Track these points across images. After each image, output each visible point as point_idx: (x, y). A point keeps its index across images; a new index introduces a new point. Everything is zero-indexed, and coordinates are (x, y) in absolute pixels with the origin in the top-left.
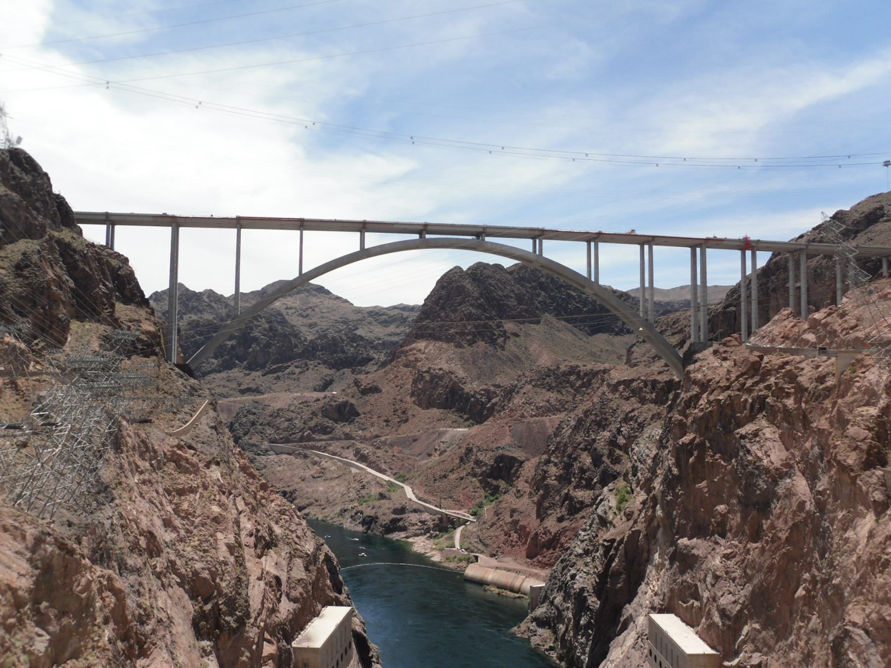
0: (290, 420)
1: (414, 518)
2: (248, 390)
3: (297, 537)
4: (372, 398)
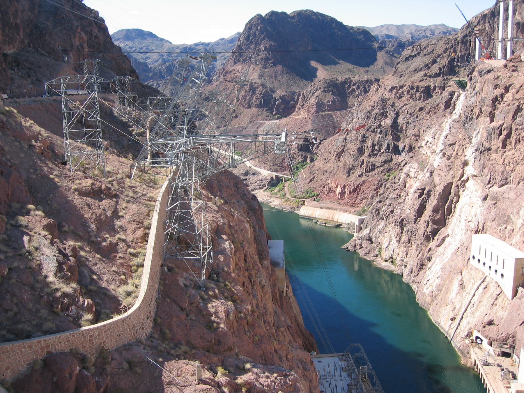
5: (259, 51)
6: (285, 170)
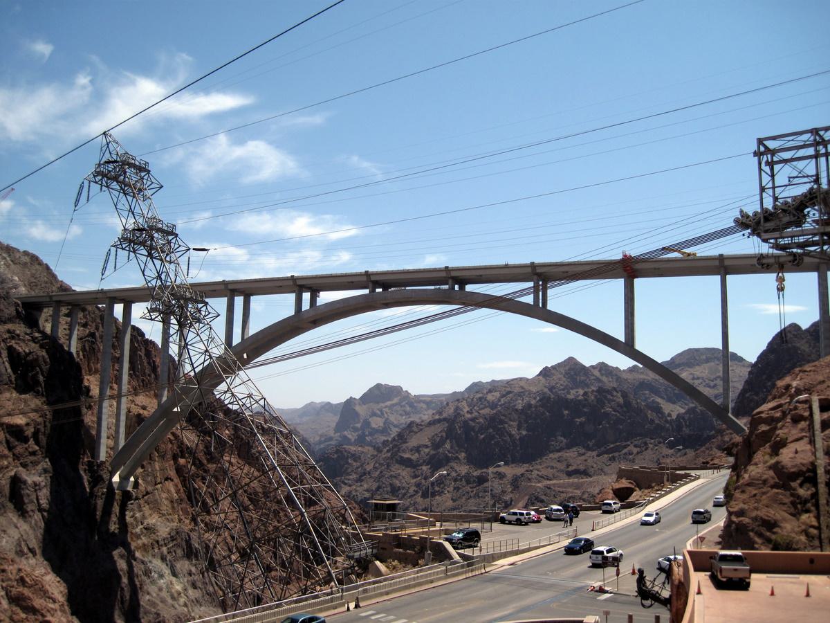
2: (577, 472)
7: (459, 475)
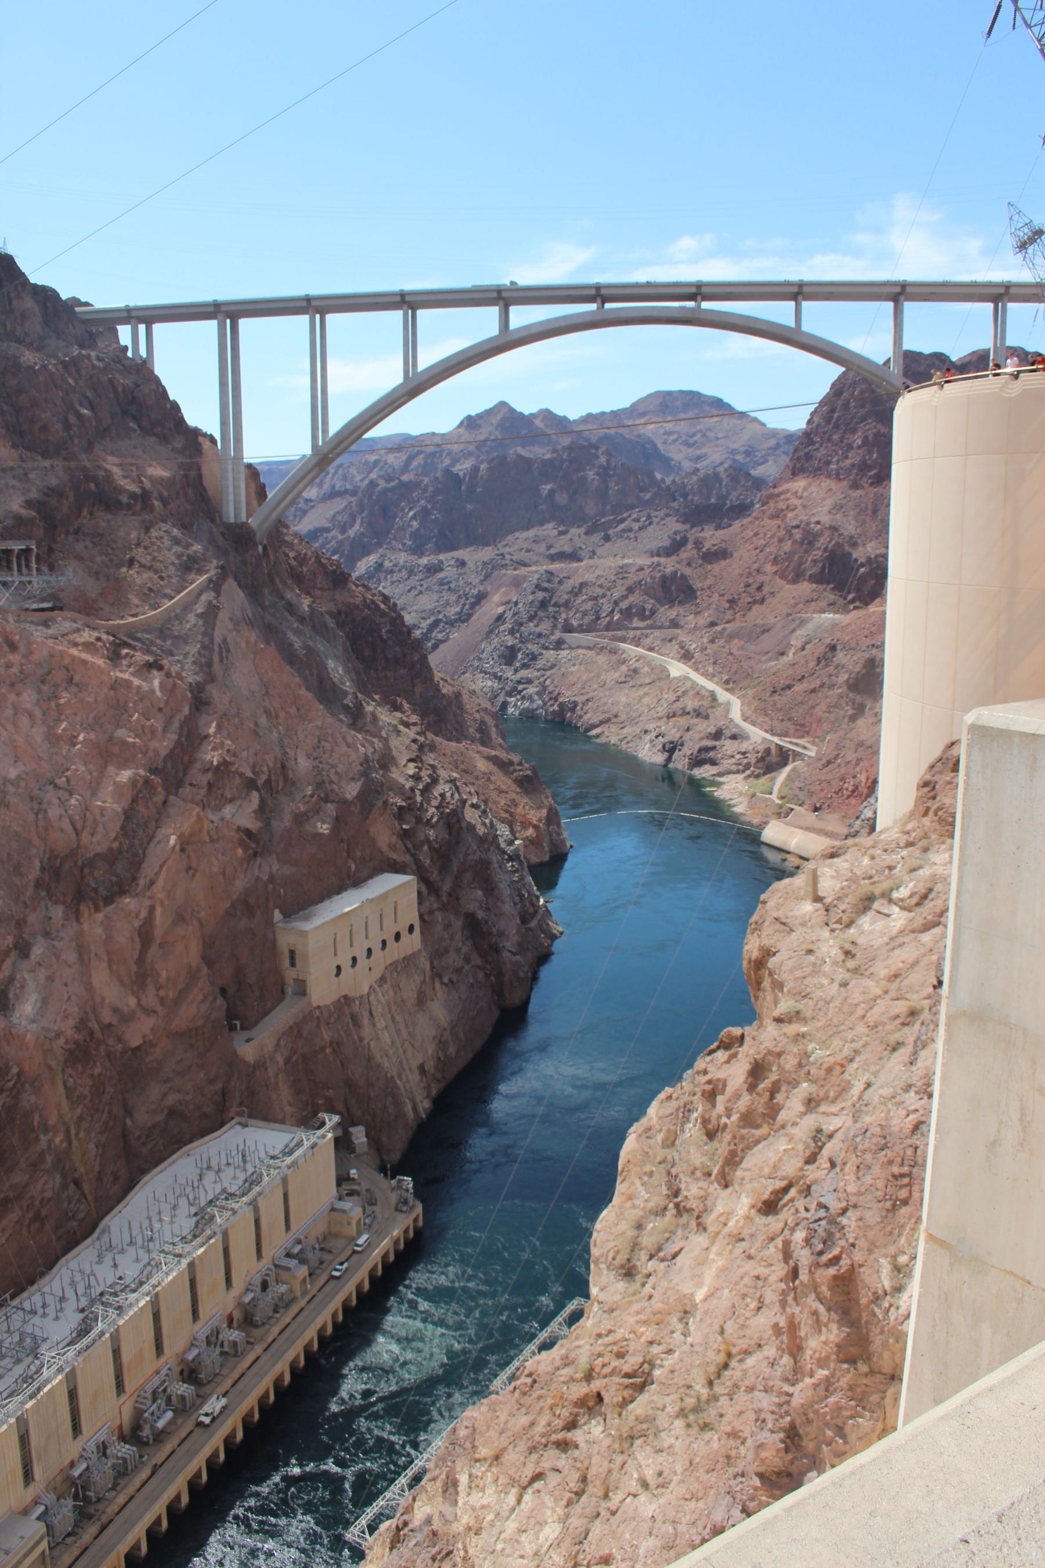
0: (595, 599)
1: (728, 747)
2: (561, 556)
3: (337, 773)
4: (716, 568)
5: (850, 447)
6: (808, 733)
7: (396, 565)
